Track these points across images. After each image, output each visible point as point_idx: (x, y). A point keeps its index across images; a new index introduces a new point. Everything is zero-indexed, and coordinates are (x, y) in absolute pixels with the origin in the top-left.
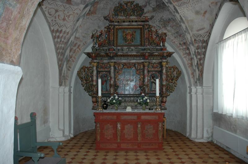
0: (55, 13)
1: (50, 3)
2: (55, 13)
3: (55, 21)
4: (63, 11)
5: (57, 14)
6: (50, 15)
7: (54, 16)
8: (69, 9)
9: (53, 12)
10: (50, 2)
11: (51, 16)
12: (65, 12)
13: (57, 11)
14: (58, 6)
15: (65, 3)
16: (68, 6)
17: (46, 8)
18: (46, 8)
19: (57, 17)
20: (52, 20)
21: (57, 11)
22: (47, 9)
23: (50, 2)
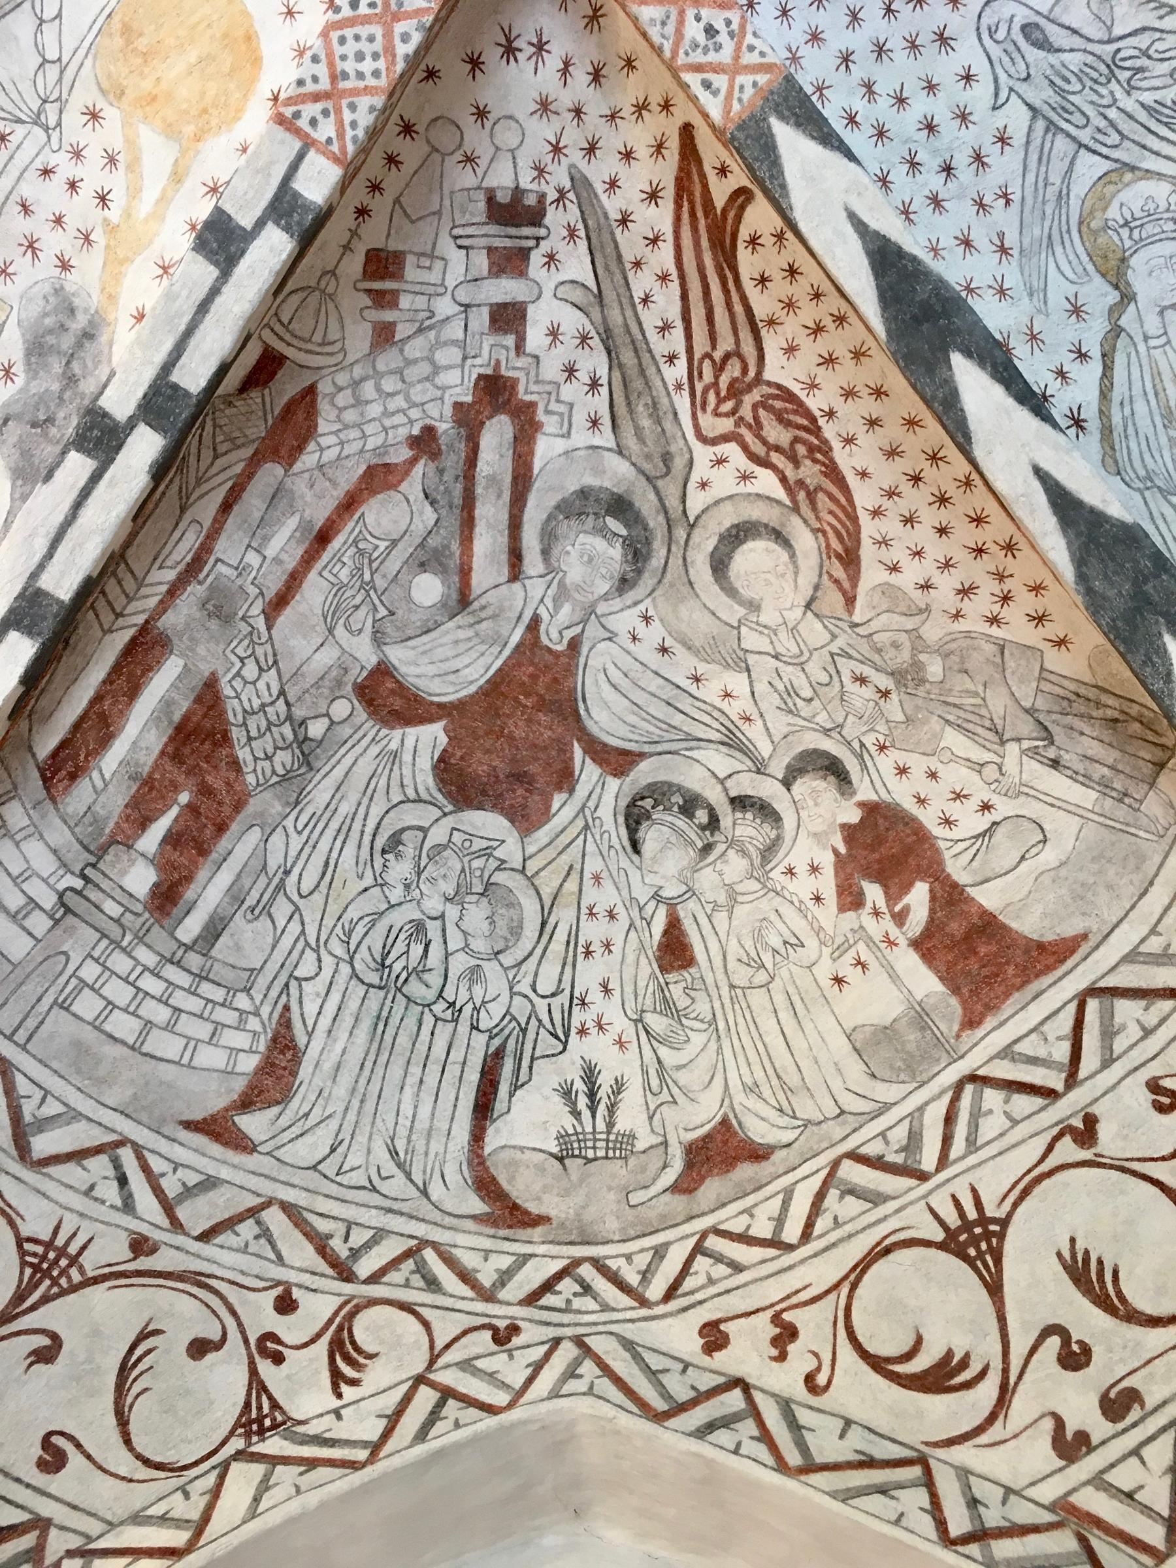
0: (995, 1289)
1: (791, 1233)
2: (995, 1289)
3: (1118, 1404)
4: (1067, 1150)
5: (1036, 1284)
6: (941, 1378)
7: (1019, 1347)
8: (1109, 1034)
9: (935, 1304)
10: (780, 1221)
11: (988, 1391)
12: (1109, 1140)
13: (976, 1242)
14: (928, 1162)
15: (971, 1022)
16: (1033, 1019)
17: (786, 1334)
18: (786, 1334)
19: (1087, 1321)
20: (1071, 1446)
21: (976, 1242)
22: (814, 1325)
23: (780, 1221)
